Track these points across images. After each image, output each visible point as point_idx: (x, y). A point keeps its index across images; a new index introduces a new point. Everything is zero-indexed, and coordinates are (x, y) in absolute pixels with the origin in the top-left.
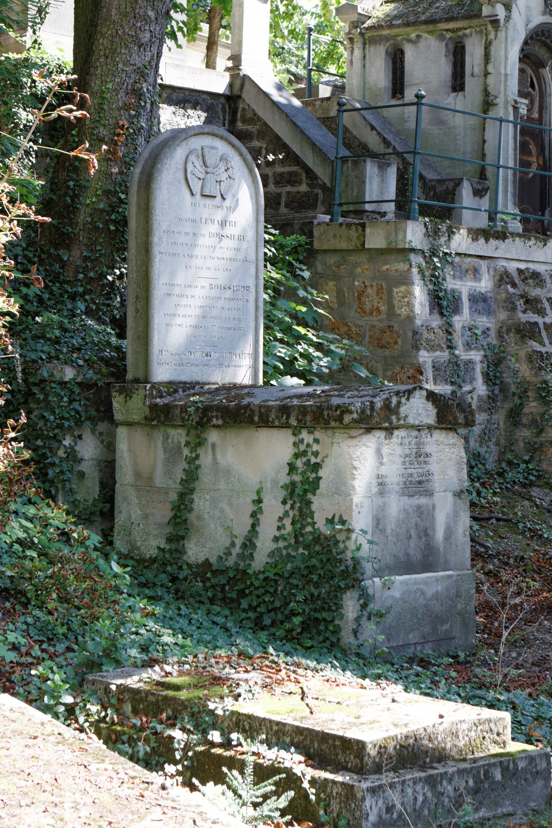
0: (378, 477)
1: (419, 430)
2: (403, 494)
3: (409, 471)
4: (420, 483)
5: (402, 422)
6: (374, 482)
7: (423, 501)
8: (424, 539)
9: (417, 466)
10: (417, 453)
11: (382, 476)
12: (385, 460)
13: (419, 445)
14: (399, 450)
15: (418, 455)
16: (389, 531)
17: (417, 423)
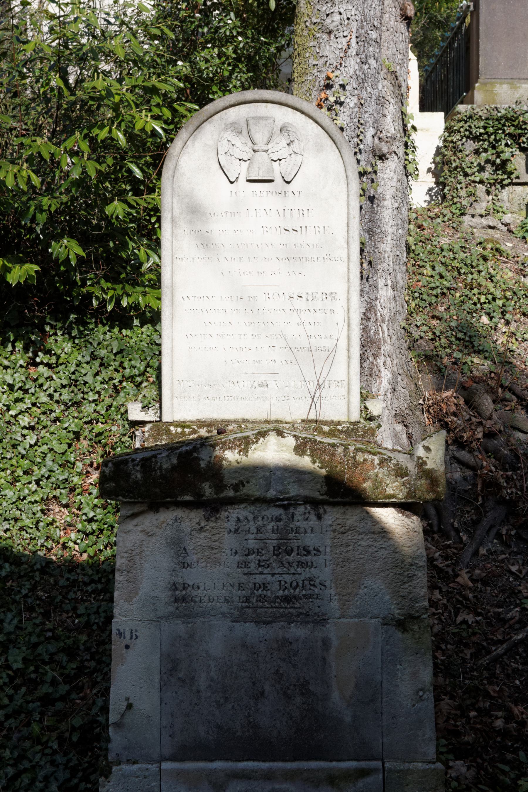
0: (174, 587)
1: (286, 508)
2: (242, 618)
3: (259, 579)
4: (287, 599)
5: (231, 493)
6: (164, 595)
7: (298, 632)
8: (298, 700)
9: (279, 570)
10: (278, 547)
11: (185, 587)
12: (193, 558)
13: (283, 534)
14: (229, 542)
15: (282, 550)
16: (202, 682)
17: (272, 493)
